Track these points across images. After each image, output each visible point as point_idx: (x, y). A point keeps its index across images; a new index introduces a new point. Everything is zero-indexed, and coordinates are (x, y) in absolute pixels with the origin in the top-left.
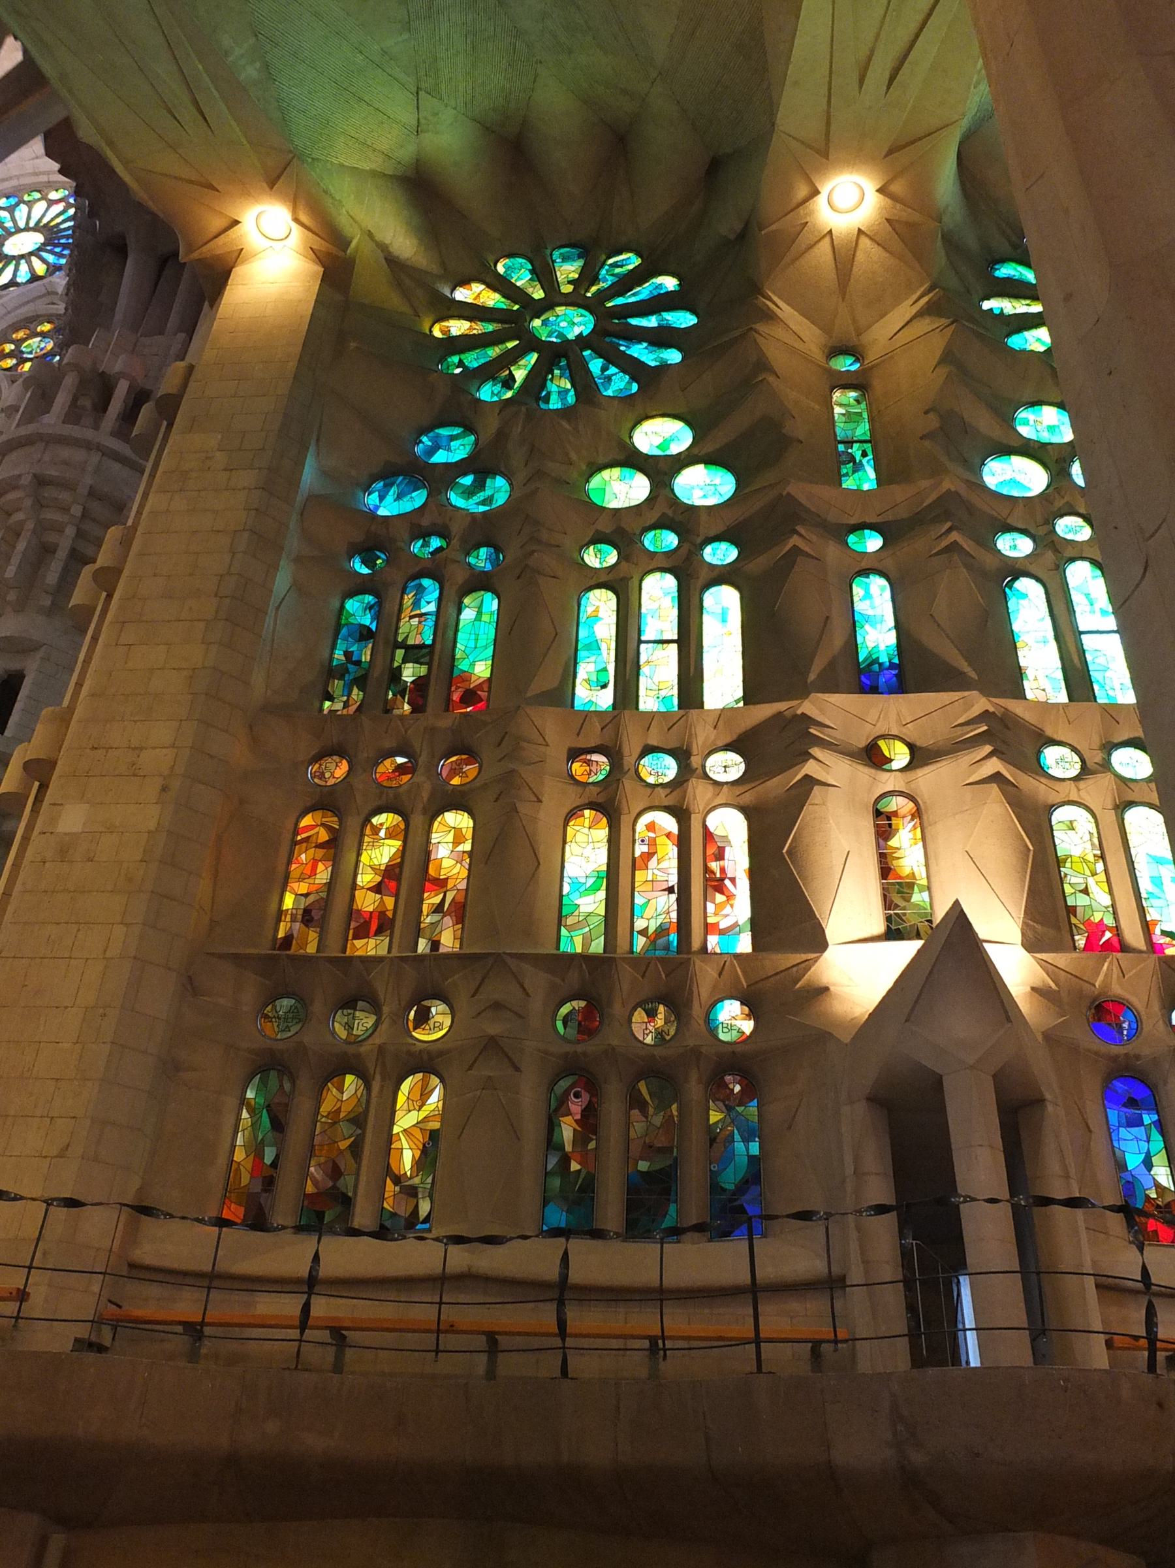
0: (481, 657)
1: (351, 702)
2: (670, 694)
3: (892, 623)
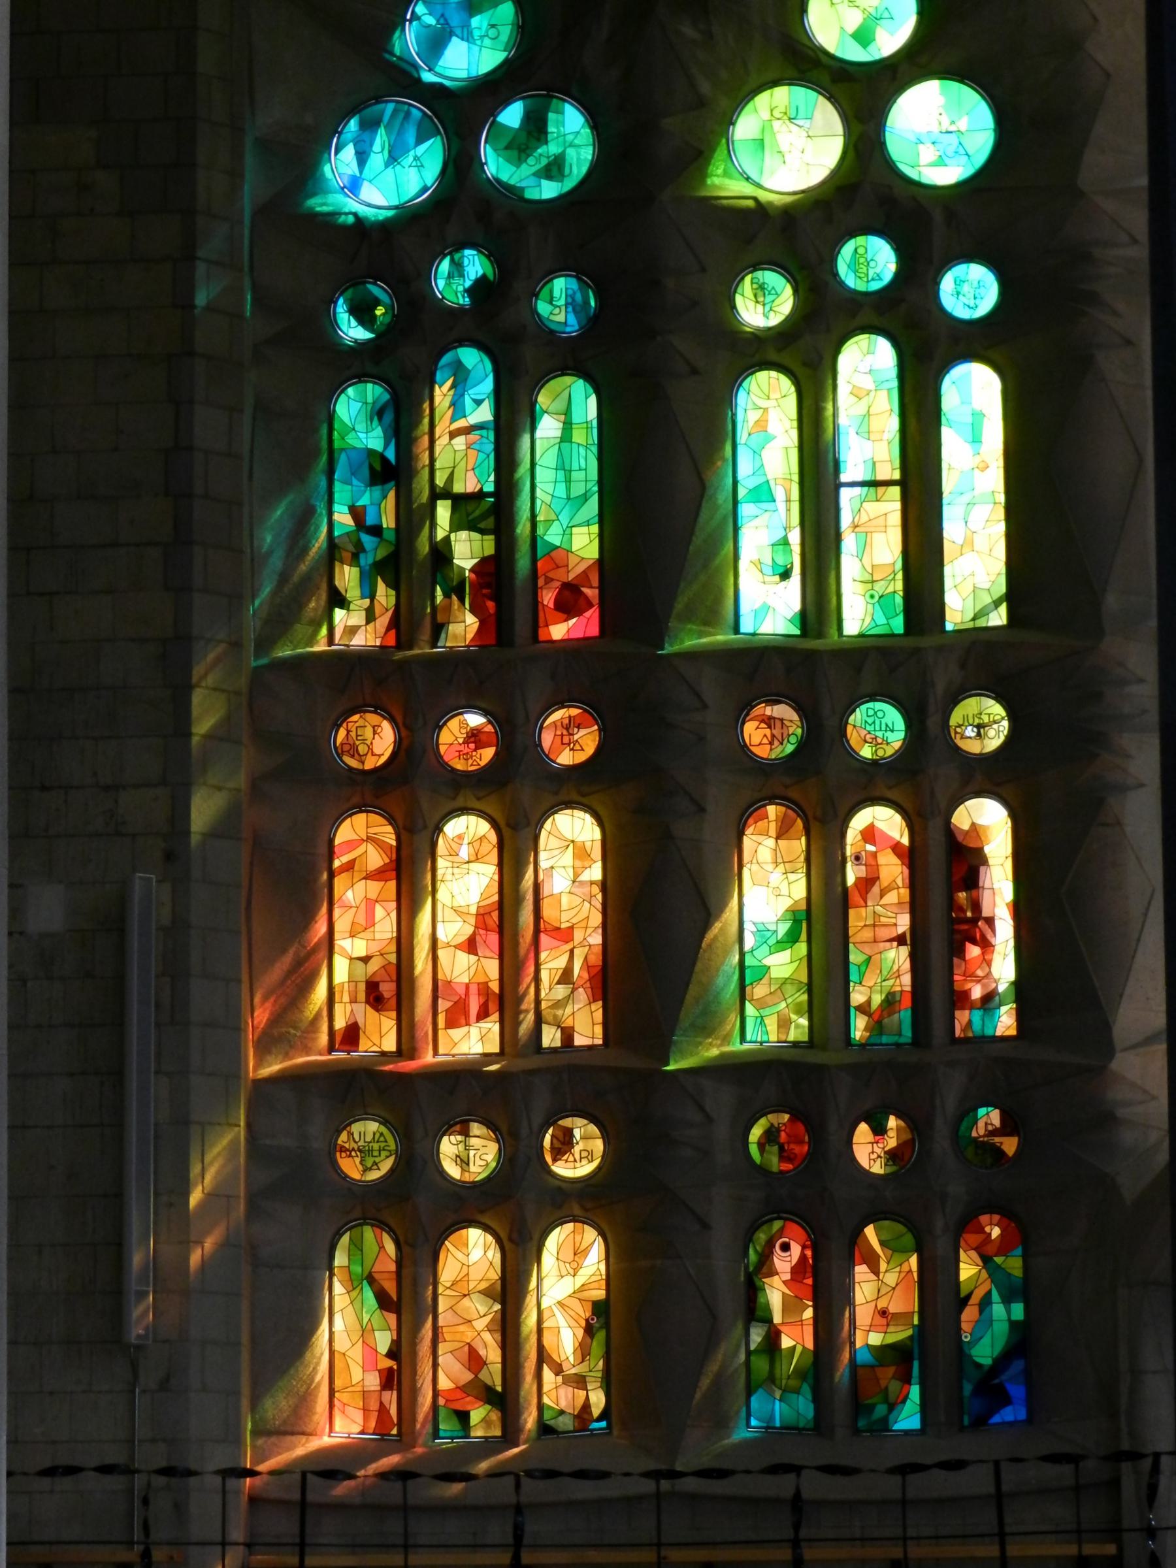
0: (579, 518)
1: (378, 610)
2: (891, 589)
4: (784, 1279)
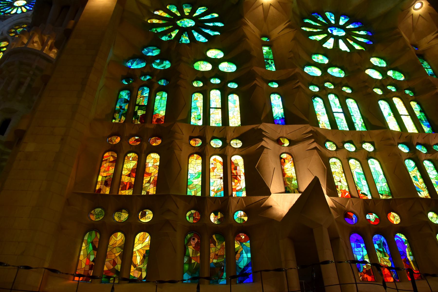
1: (121, 120)
2: (219, 122)
3: (282, 107)
4: (193, 246)
